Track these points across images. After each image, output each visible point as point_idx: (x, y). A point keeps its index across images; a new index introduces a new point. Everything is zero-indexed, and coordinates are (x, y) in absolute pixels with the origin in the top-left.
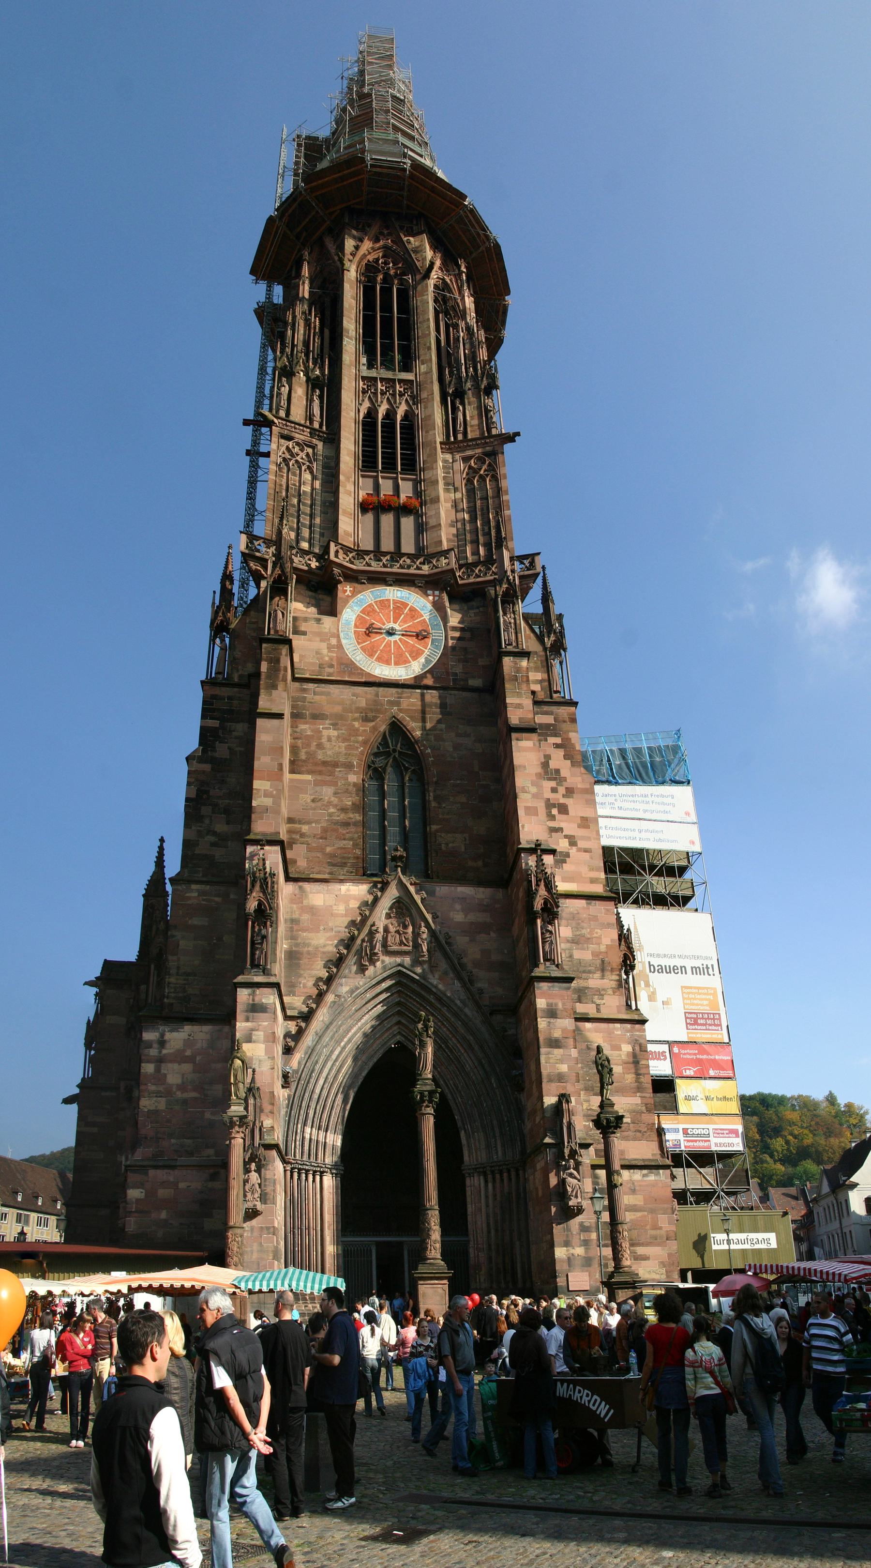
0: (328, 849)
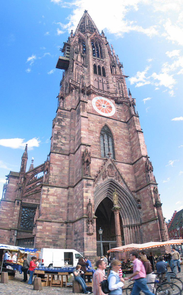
0: (92, 150)
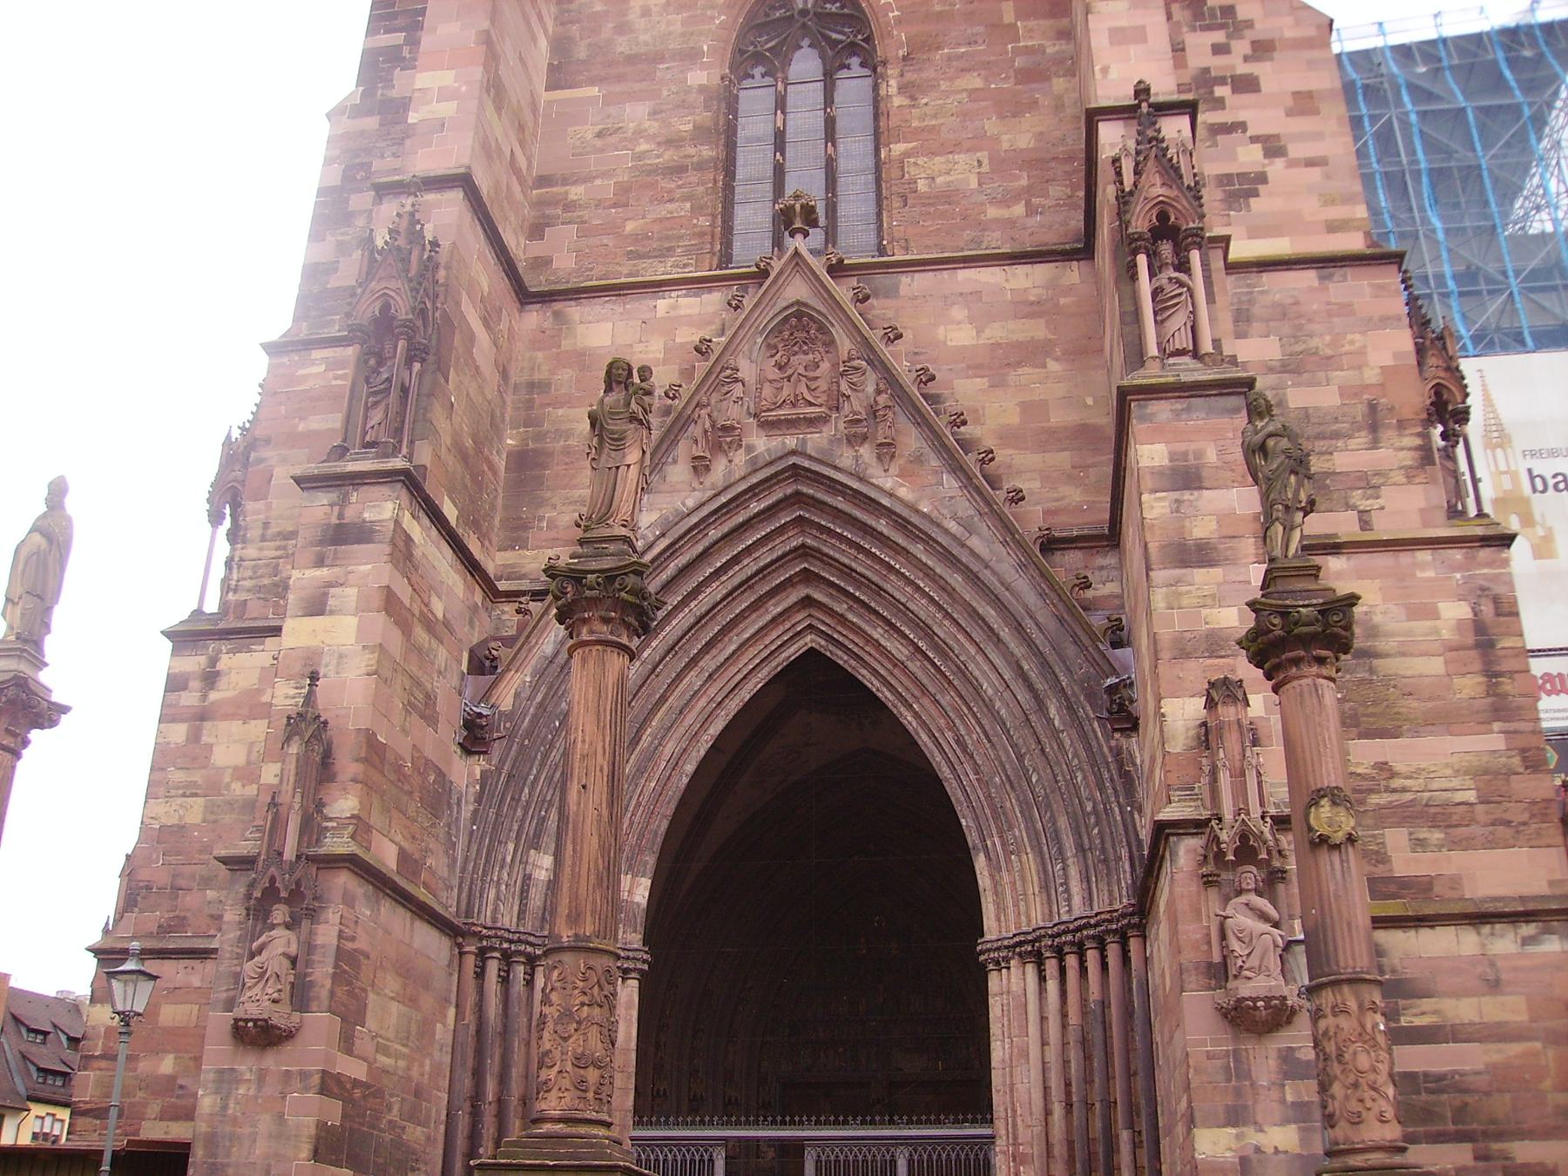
0: (630, 227)
